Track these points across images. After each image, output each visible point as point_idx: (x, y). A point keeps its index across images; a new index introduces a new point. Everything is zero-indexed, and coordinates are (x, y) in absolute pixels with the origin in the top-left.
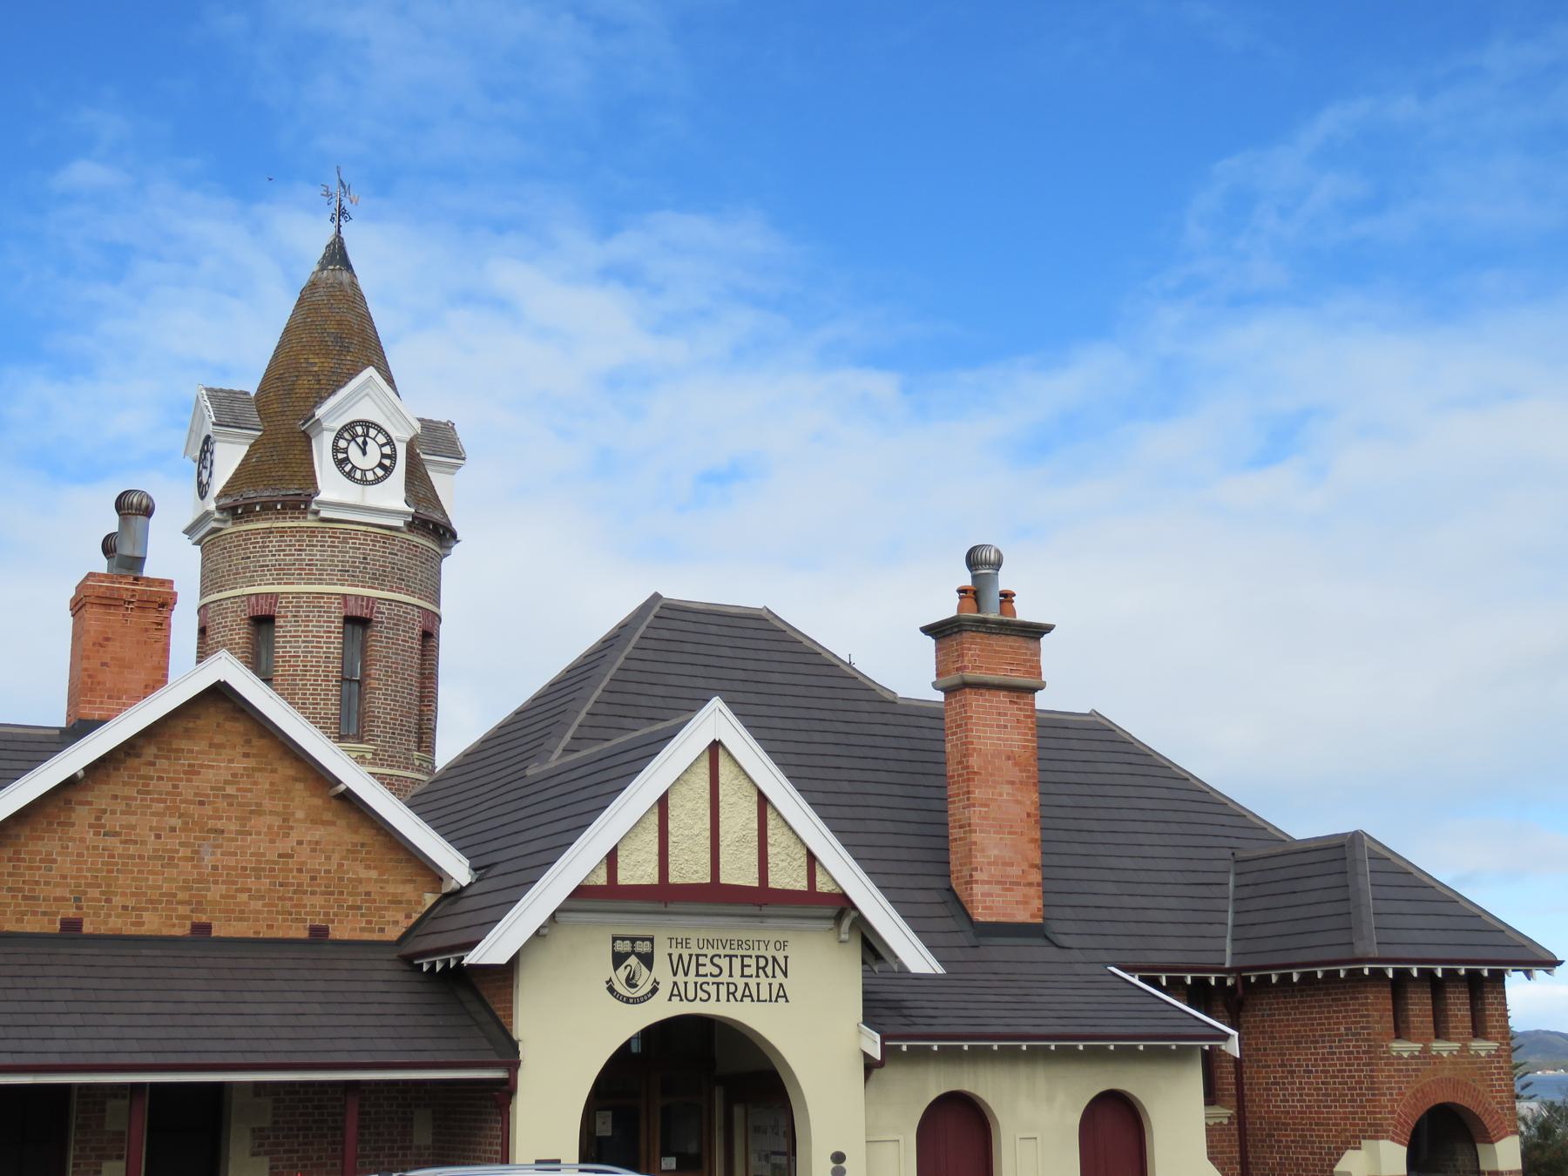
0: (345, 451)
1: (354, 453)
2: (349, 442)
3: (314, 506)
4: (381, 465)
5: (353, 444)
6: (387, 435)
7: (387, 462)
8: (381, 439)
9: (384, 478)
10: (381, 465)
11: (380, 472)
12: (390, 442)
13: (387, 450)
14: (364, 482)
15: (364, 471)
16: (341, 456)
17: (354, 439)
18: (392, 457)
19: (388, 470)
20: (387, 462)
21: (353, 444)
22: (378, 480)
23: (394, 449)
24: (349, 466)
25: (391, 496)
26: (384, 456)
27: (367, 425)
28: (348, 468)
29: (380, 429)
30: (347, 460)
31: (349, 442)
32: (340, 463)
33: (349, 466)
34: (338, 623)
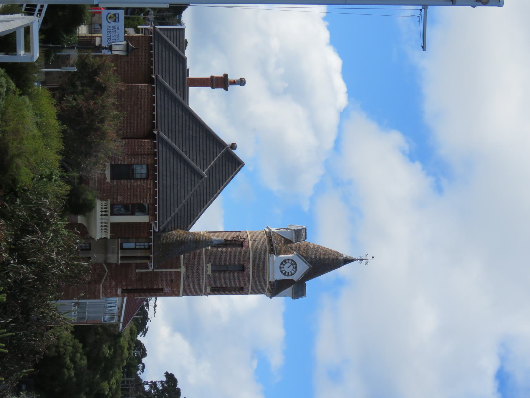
0: (288, 262)
1: (287, 265)
2: (291, 263)
3: (272, 255)
4: (286, 272)
5: (290, 264)
6: (294, 273)
7: (287, 274)
8: (293, 272)
9: (282, 273)
10: (286, 272)
11: (284, 272)
12: (292, 274)
13: (290, 274)
14: (281, 268)
15: (283, 267)
16: (287, 261)
17: (292, 264)
18: (288, 275)
19: (284, 274)
20: (287, 274)
21: (290, 264)
22: (281, 271)
23: (290, 276)
24: (284, 264)
25: (278, 276)
26: (288, 273)
27: (296, 268)
28: (284, 263)
29: (295, 272)
30: (286, 263)
31: (291, 263)
32: (285, 261)
33: (284, 264)
34: (243, 263)
